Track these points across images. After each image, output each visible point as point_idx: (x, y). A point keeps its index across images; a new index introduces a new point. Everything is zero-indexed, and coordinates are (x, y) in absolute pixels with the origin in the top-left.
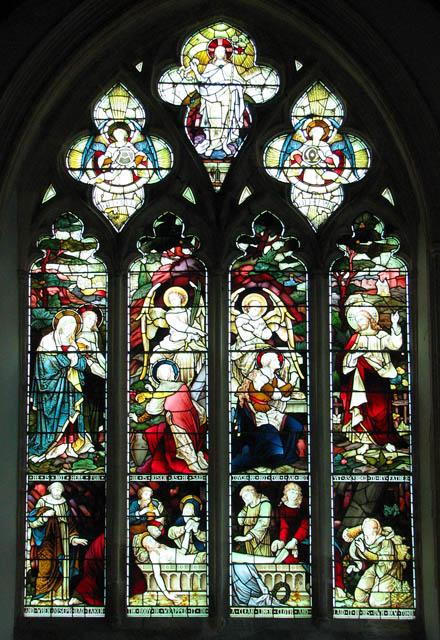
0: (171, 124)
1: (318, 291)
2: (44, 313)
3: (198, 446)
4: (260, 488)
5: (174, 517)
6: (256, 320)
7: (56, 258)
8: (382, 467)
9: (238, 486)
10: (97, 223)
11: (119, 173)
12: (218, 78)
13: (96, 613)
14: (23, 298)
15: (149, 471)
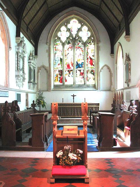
0: (69, 30)
1: (85, 49)
2: (55, 52)
3: (72, 66)
4: (79, 70)
5: (70, 73)
6: (78, 52)
7: (57, 45)
10: (61, 42)
11: (63, 34)
12: (74, 24)
13: (62, 84)
14: (54, 50)
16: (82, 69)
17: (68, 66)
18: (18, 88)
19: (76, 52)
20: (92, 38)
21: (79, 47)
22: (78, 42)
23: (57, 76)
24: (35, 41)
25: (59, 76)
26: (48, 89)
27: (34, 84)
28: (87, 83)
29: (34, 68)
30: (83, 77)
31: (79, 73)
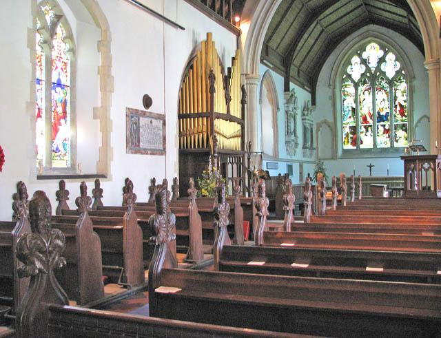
3: (371, 119)
4: (382, 125)
5: (367, 131)
6: (381, 96)
7: (346, 87)
8: (402, 121)
10: (353, 81)
11: (356, 70)
12: (373, 52)
13: (355, 148)
16: (387, 124)
17: (365, 119)
18: (289, 157)
19: (377, 96)
20: (403, 72)
21: (381, 89)
22: (380, 80)
23: (347, 135)
24: (311, 83)
25: (351, 136)
26: (334, 157)
27: (312, 148)
28: (396, 145)
29: (311, 125)
31: (381, 129)
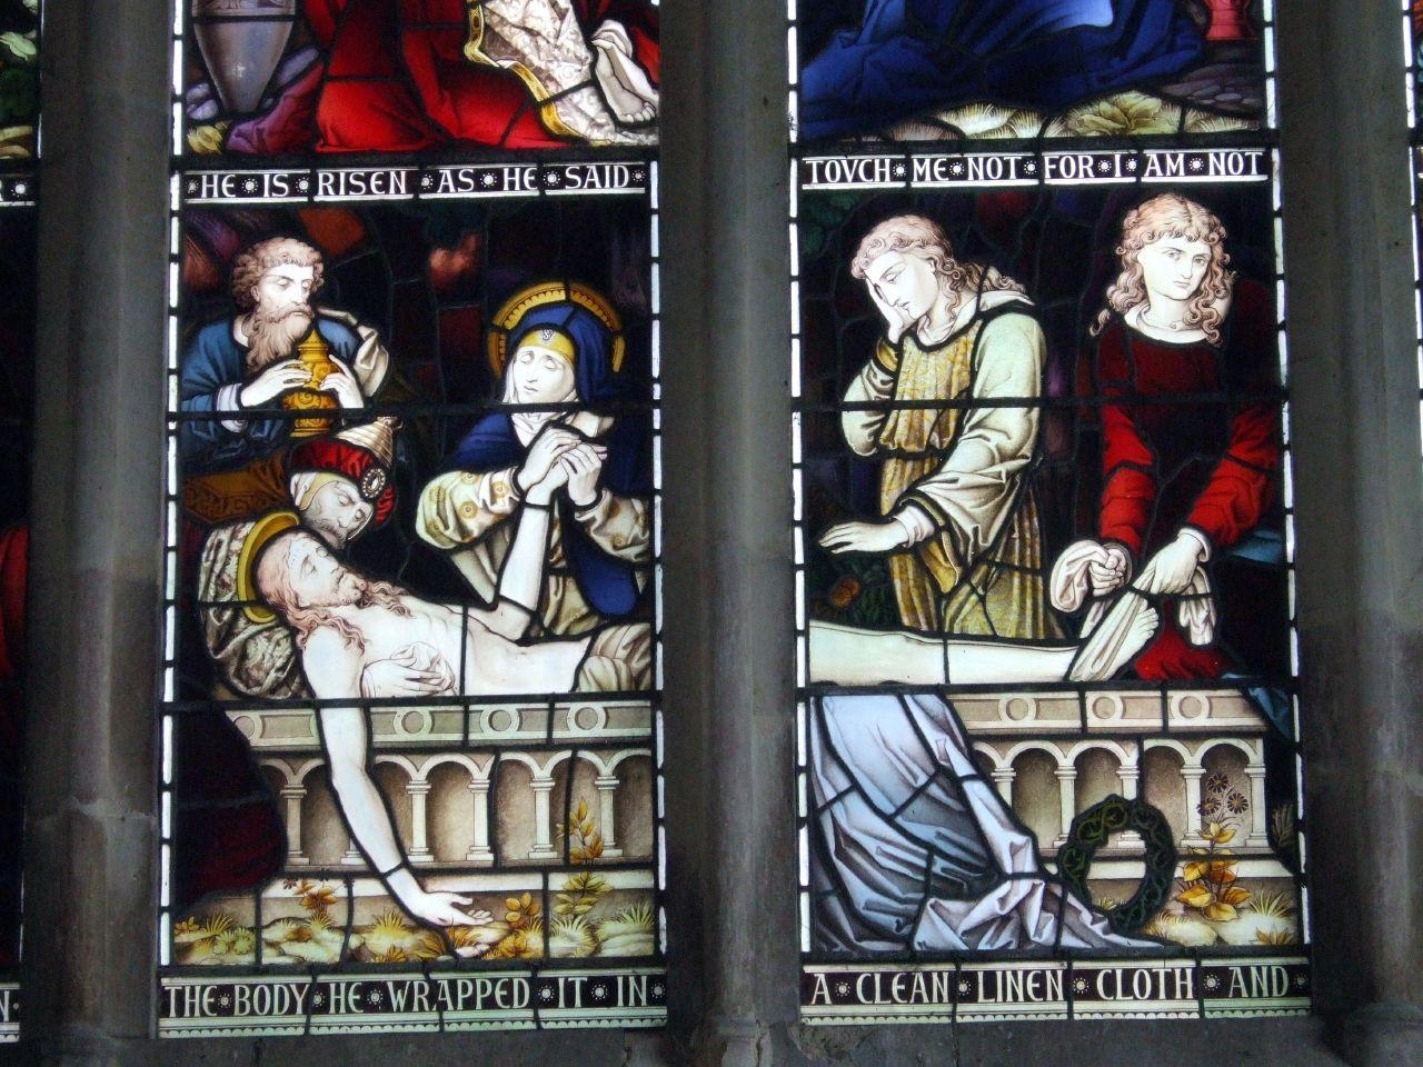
4: (973, 233)
5: (450, 412)
9: (840, 226)
15: (302, 146)
30: (1240, 586)
